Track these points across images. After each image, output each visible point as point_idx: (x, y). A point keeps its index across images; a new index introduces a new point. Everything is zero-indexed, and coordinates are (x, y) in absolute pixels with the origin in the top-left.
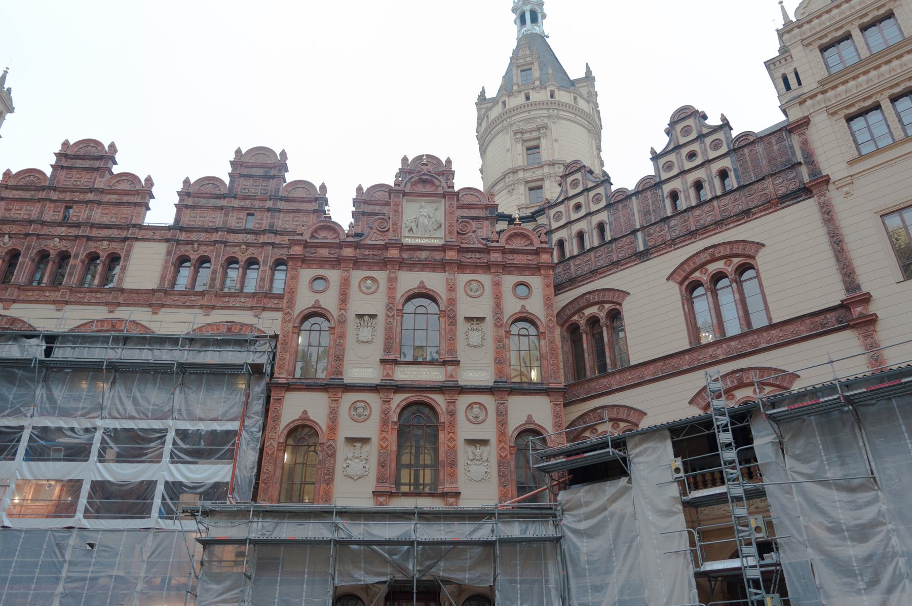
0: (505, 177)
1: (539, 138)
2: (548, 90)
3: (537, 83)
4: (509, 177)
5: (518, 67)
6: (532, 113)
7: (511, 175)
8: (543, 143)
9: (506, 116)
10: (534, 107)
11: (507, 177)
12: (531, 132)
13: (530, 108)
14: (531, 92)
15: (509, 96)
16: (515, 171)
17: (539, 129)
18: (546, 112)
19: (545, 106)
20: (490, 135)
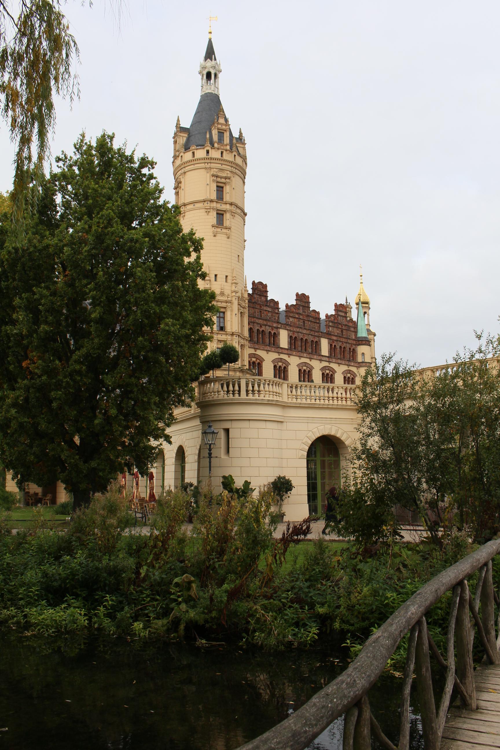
0: (205, 201)
1: (224, 183)
2: (233, 154)
3: (228, 148)
4: (208, 203)
6: (223, 166)
7: (209, 202)
8: (227, 189)
10: (225, 163)
11: (206, 202)
13: (222, 162)
15: (212, 148)
16: (212, 201)
17: (226, 178)
18: (230, 168)
19: (230, 164)
20: (192, 166)
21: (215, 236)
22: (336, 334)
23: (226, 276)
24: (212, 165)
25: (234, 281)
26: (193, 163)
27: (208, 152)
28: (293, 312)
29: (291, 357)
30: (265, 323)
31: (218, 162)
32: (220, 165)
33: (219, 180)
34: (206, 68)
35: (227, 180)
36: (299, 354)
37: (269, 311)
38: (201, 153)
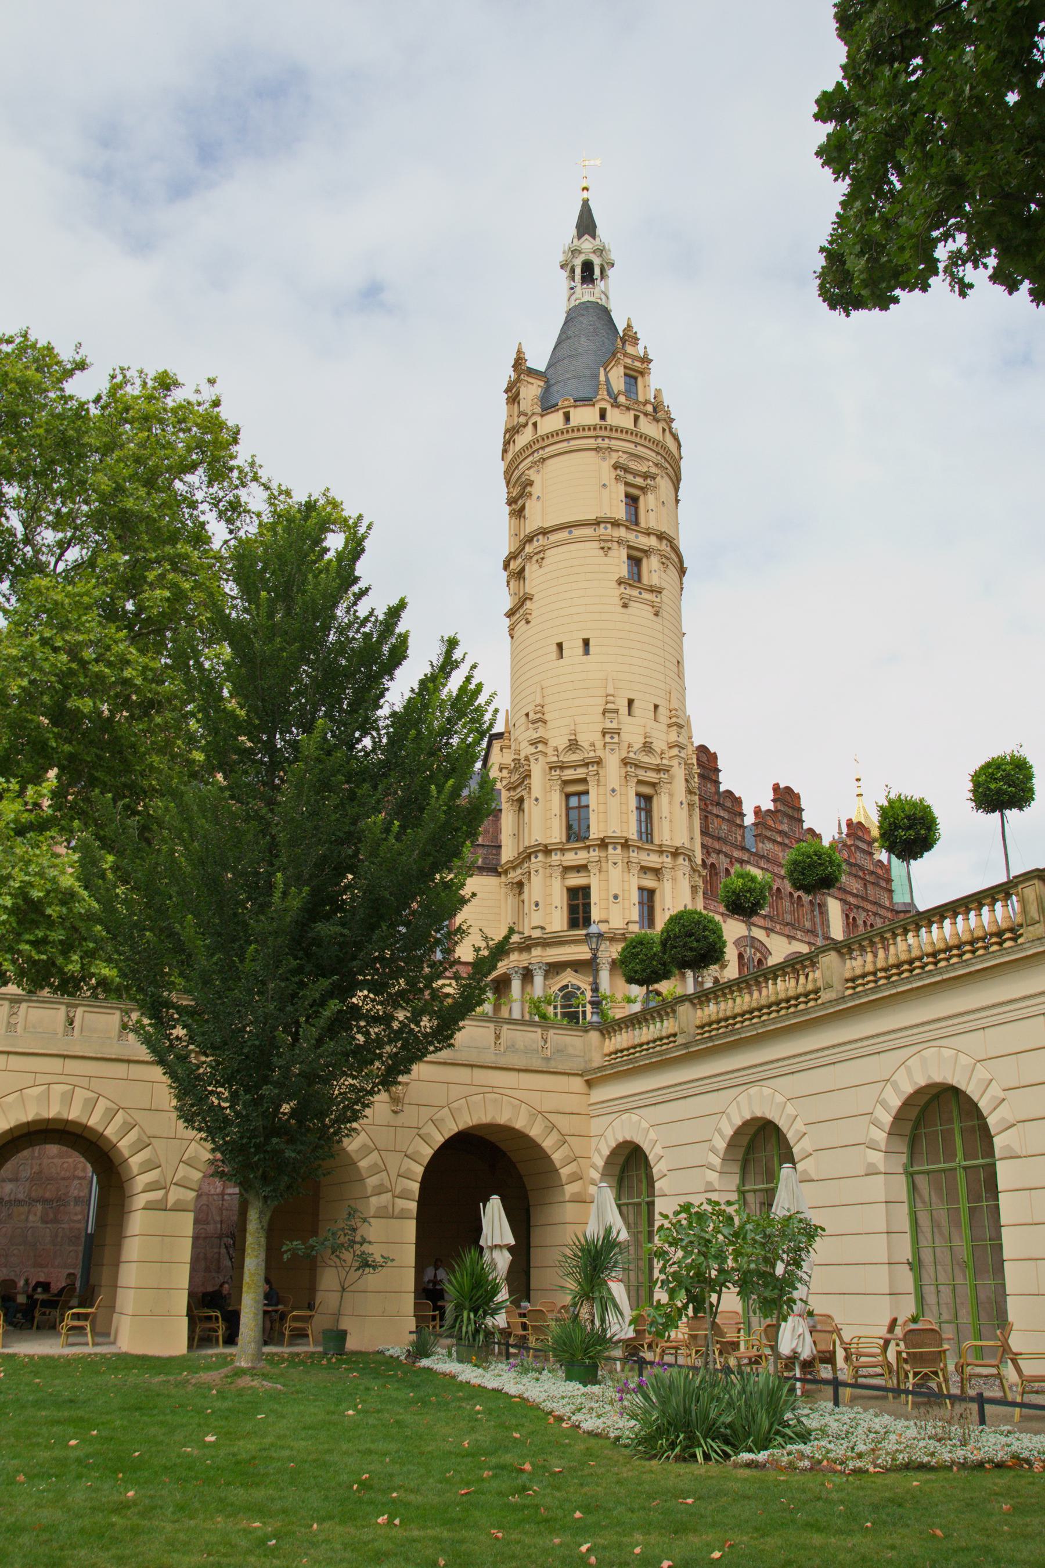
5: (625, 367)
6: (639, 448)
7: (609, 526)
9: (599, 433)
10: (642, 442)
11: (602, 526)
12: (635, 474)
13: (638, 440)
14: (642, 416)
15: (612, 406)
16: (616, 524)
17: (645, 476)
18: (653, 454)
20: (565, 444)
21: (625, 606)
22: (855, 891)
23: (656, 707)
24: (613, 442)
25: (674, 720)
26: (566, 436)
27: (603, 415)
28: (770, 828)
29: (773, 935)
30: (717, 846)
31: (628, 437)
32: (632, 446)
33: (630, 478)
34: (580, 252)
35: (649, 481)
36: (787, 930)
37: (723, 818)
38: (585, 416)
